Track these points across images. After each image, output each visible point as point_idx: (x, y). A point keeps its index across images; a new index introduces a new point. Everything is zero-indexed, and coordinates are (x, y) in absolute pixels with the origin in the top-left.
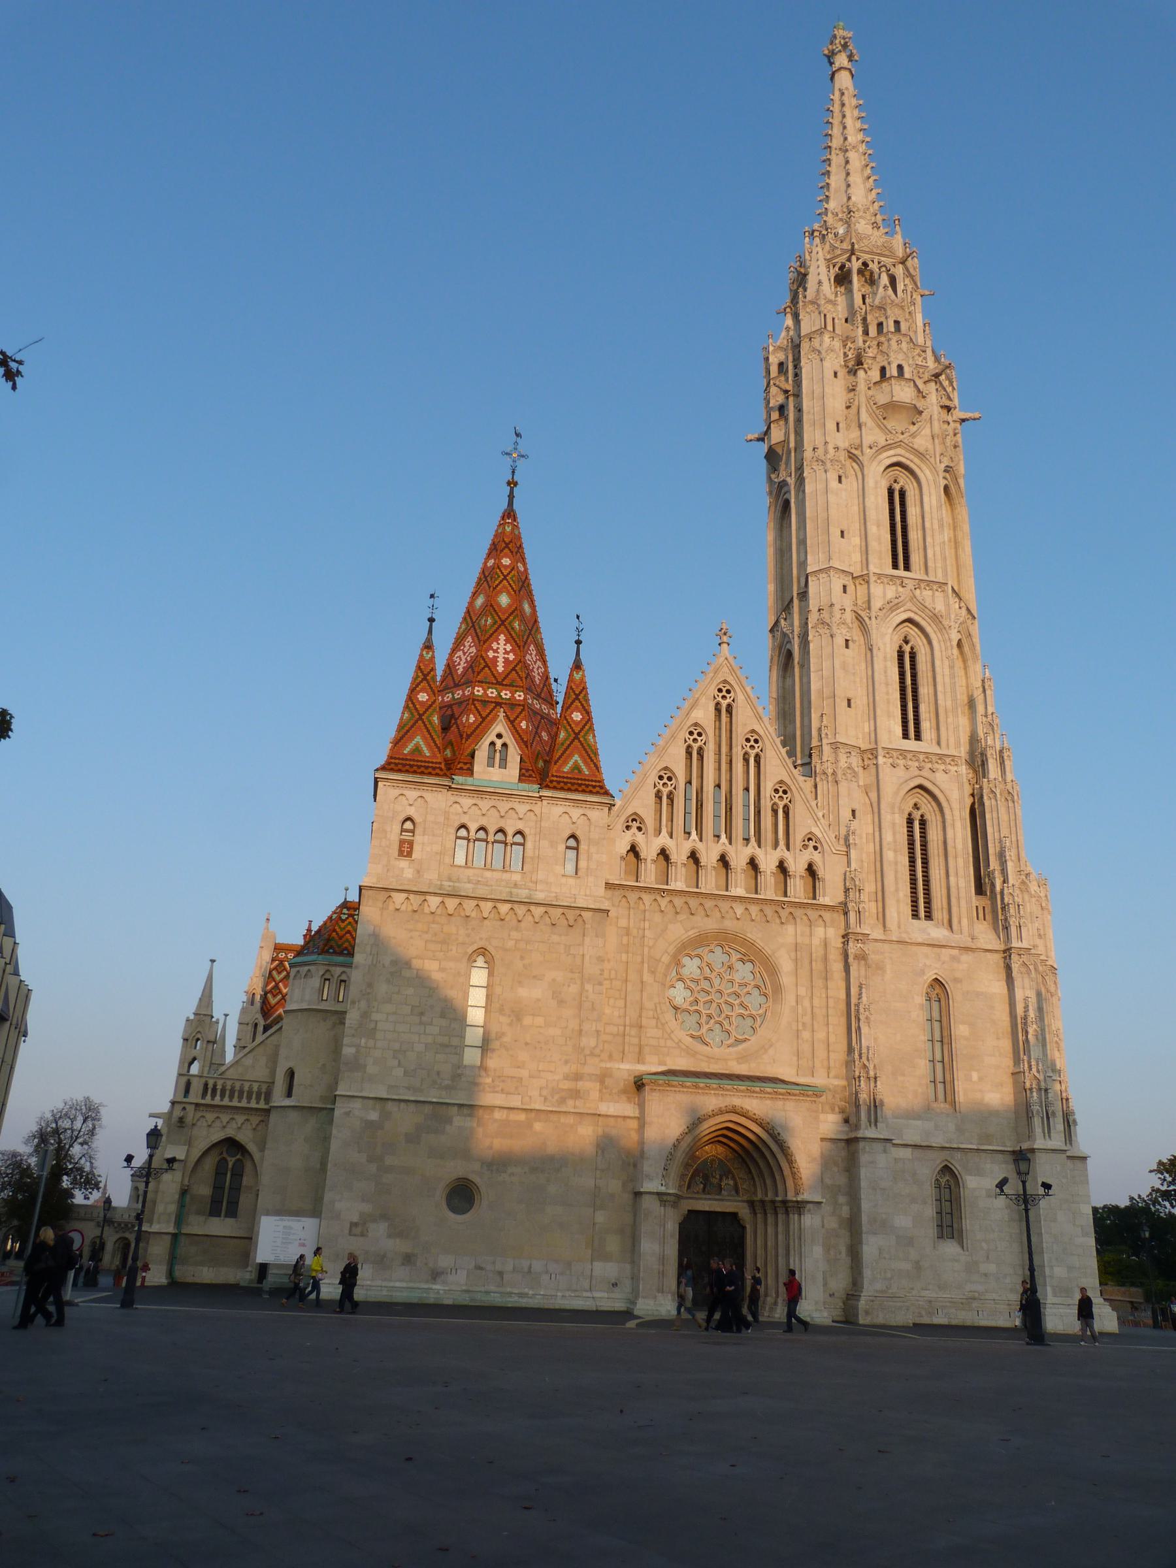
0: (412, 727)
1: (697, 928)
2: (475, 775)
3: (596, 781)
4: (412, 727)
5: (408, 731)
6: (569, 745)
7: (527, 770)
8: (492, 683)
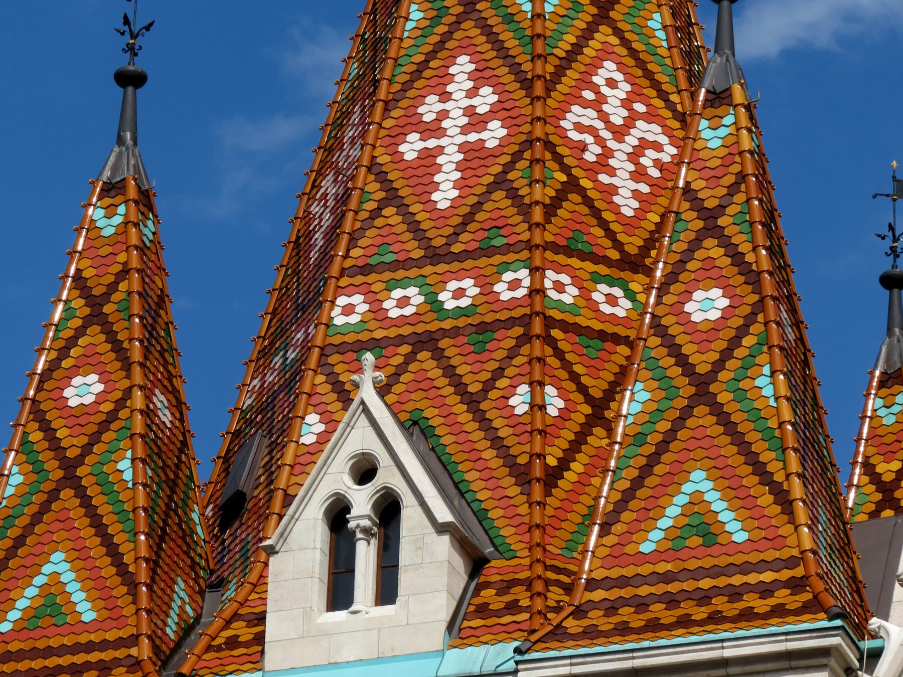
0: (37, 519)
4: (37, 519)
5: (19, 541)
6: (670, 436)
7: (506, 587)
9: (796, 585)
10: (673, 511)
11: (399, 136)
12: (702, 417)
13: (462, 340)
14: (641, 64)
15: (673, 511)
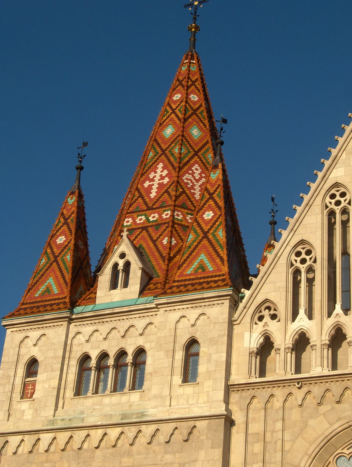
0: (47, 270)
1: (344, 418)
2: (98, 301)
3: (219, 276)
4: (47, 270)
6: (197, 246)
8: (143, 211)
9: (223, 280)
10: (196, 264)
11: (144, 182)
12: (205, 241)
14: (204, 165)
15: (196, 264)
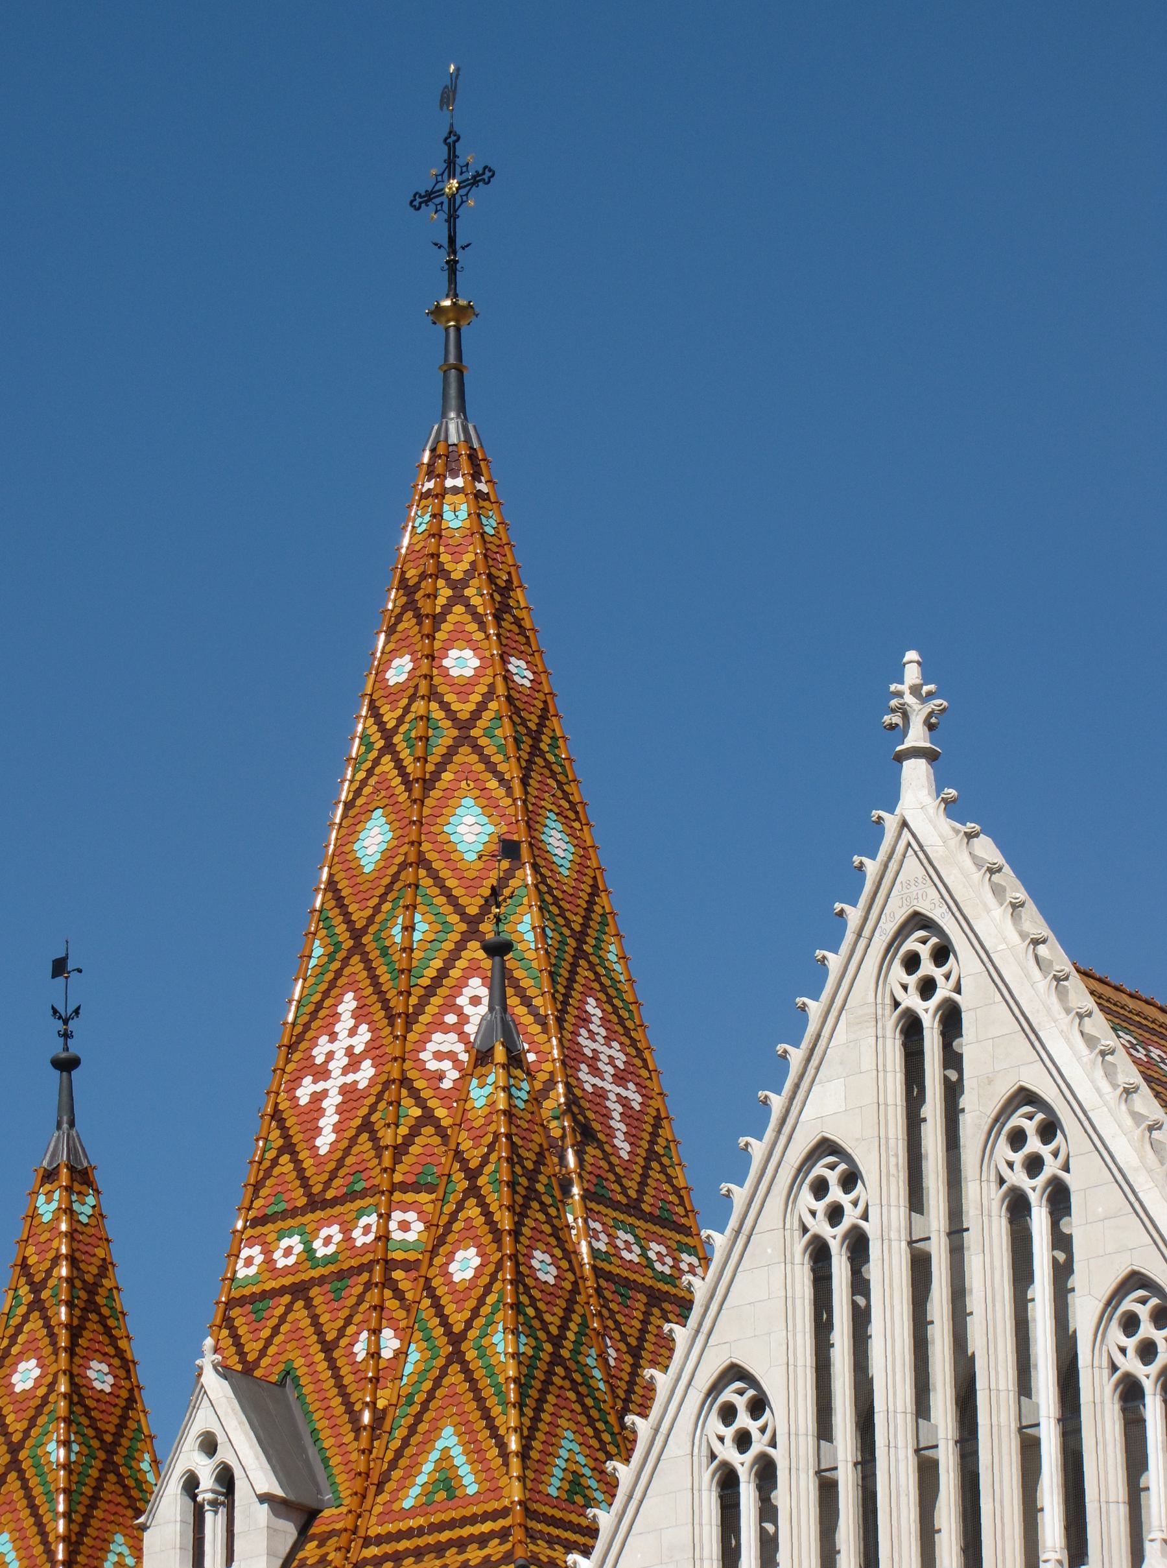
8: (293, 1213)
9: (504, 1534)
10: (428, 1467)
11: (296, 1081)
13: (327, 1287)
15: (428, 1467)
